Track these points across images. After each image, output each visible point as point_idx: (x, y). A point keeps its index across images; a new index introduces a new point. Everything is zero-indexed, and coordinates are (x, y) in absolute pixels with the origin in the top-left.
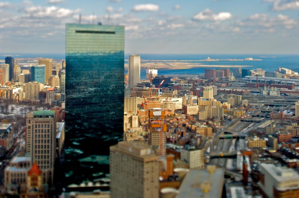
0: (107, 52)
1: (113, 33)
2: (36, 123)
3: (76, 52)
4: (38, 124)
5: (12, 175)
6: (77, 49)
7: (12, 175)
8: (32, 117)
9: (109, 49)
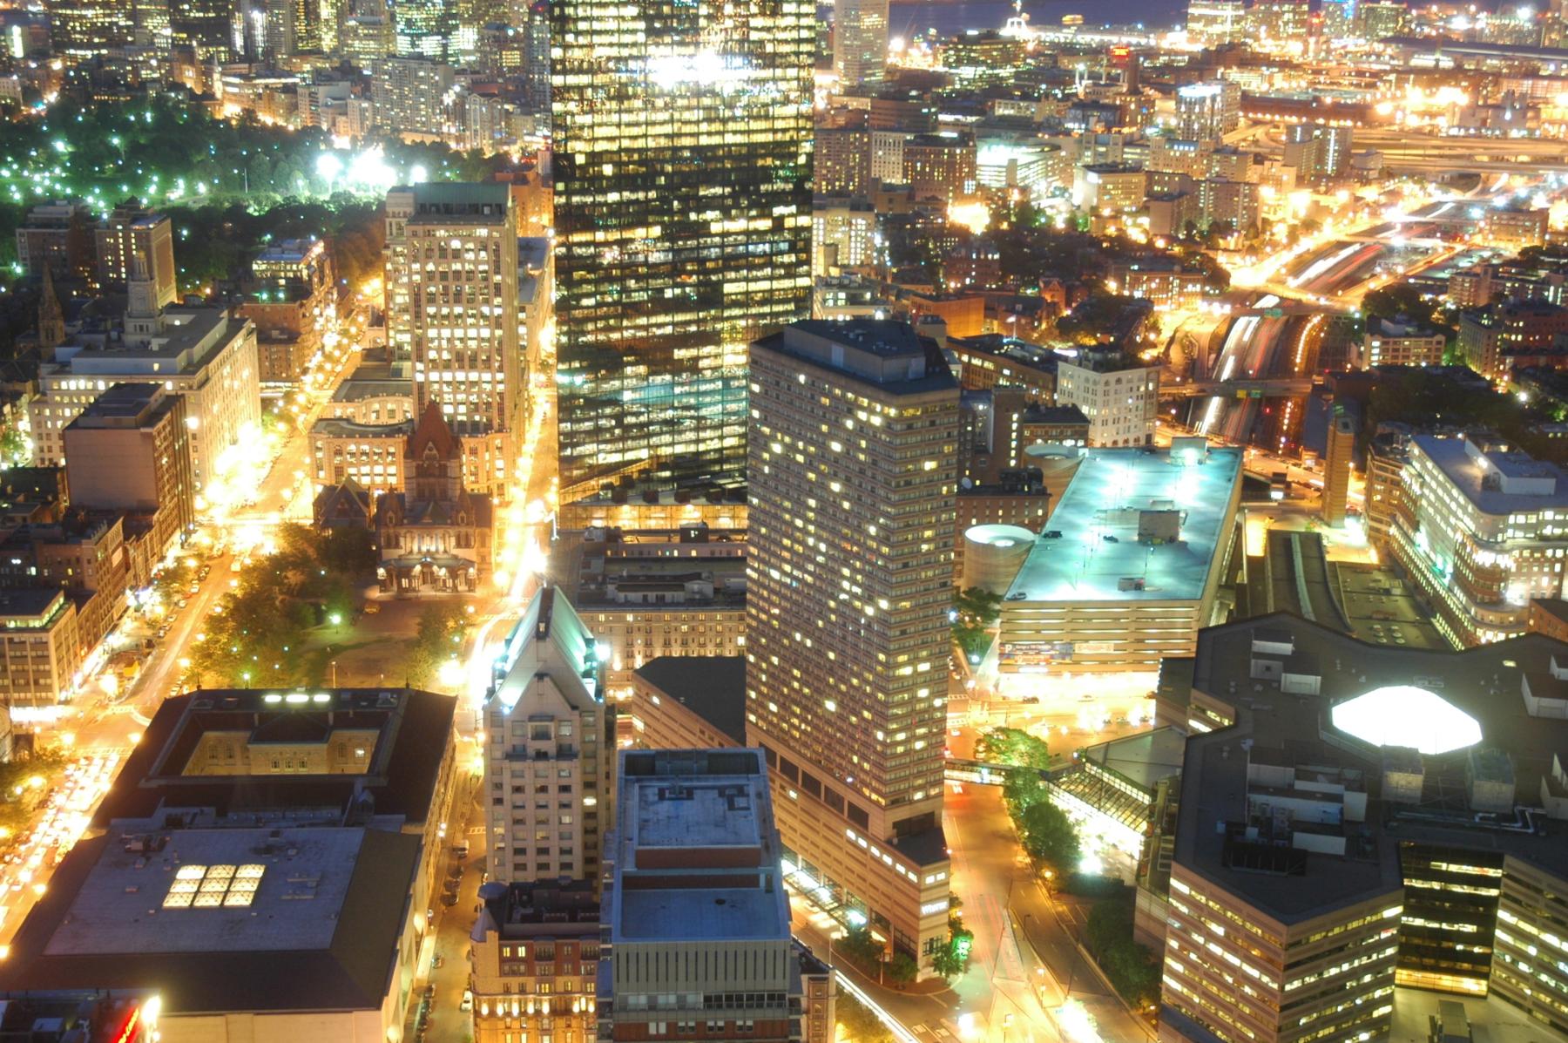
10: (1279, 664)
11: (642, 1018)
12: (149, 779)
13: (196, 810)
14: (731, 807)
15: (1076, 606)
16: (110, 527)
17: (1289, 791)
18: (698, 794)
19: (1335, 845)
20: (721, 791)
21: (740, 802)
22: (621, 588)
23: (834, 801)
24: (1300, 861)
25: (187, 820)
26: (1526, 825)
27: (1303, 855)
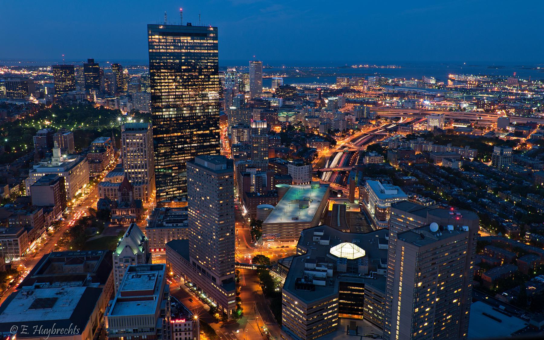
10: (319, 238)
11: (117, 336)
13: (44, 283)
14: (150, 280)
15: (281, 224)
16: (39, 211)
17: (314, 270)
19: (323, 283)
22: (166, 223)
23: (209, 275)
24: (313, 287)
26: (371, 276)
27: (314, 285)
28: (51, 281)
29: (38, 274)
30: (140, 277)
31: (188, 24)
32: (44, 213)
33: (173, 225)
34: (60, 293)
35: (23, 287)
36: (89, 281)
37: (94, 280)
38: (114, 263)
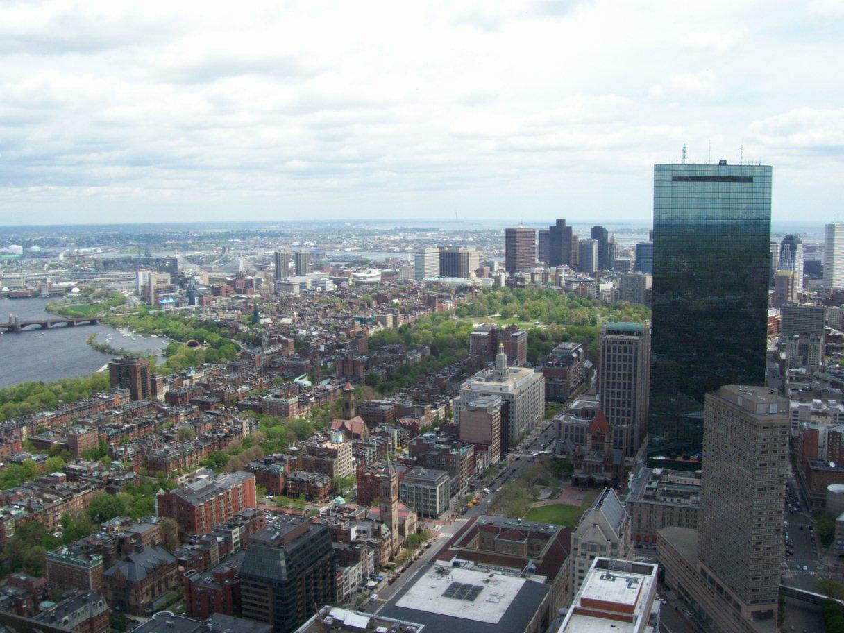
0: (734, 217)
1: (750, 179)
2: (609, 344)
3: (674, 216)
4: (612, 345)
5: (567, 428)
6: (675, 211)
7: (567, 428)
8: (604, 333)
9: (739, 212)
12: (452, 547)
13: (467, 561)
18: (617, 579)
20: (628, 580)
21: (633, 585)
25: (462, 565)
28: (479, 559)
29: (459, 545)
30: (614, 580)
31: (721, 161)
32: (475, 454)
33: (672, 500)
34: (487, 581)
35: (437, 561)
36: (531, 571)
37: (539, 571)
38: (572, 549)
